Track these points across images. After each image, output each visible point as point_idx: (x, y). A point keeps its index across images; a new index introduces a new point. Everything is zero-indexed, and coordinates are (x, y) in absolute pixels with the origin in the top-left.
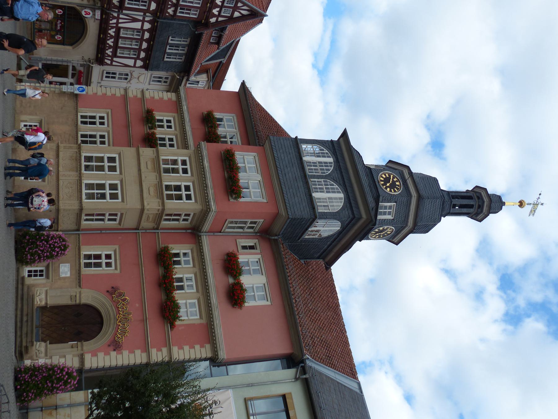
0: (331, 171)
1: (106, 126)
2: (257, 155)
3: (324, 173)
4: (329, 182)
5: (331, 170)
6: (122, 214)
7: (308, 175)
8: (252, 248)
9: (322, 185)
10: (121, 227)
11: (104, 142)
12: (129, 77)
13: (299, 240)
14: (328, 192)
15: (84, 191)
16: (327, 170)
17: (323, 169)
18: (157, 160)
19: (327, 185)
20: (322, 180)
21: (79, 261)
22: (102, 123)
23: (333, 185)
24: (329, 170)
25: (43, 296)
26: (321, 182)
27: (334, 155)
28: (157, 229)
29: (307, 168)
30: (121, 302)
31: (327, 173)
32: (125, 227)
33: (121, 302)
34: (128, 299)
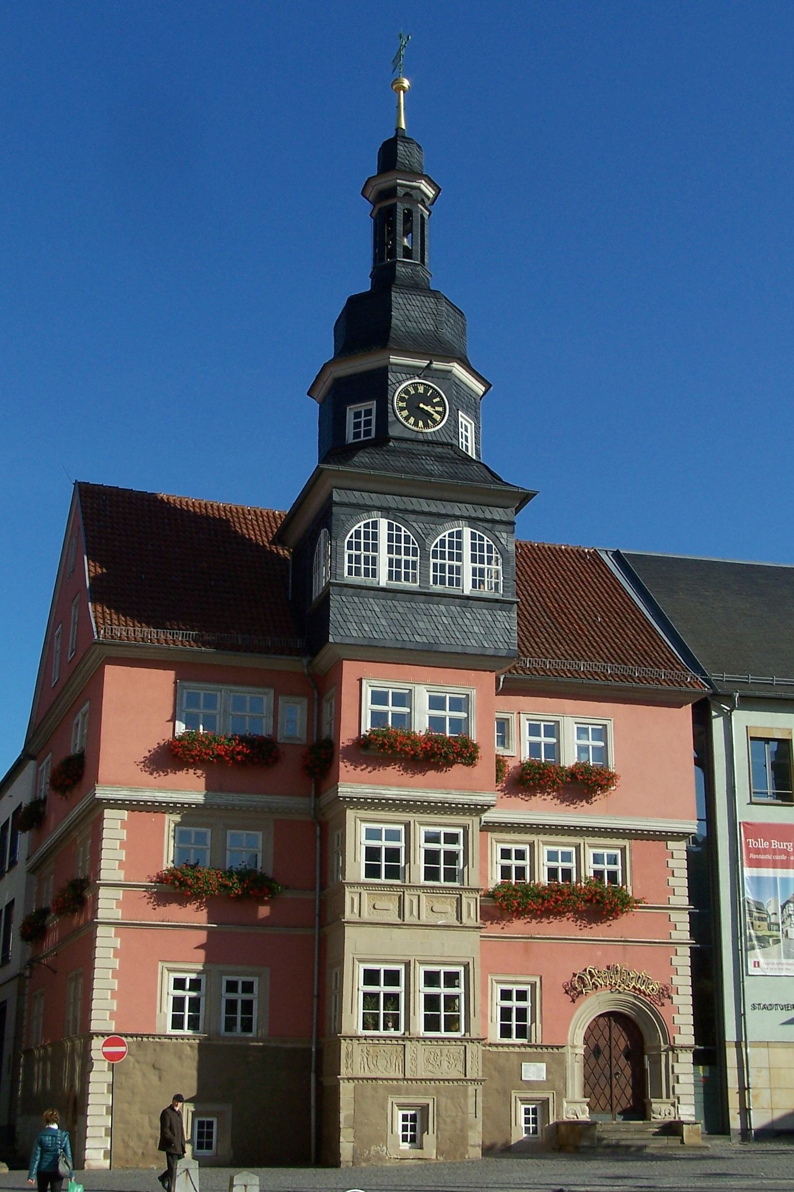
0: (409, 533)
2: (368, 681)
4: (436, 546)
5: (406, 530)
16: (407, 541)
20: (431, 559)
21: (513, 1045)
24: (407, 538)
25: (577, 1107)
27: (368, 511)
30: (595, 980)
31: (414, 543)
33: (595, 980)
34: (591, 968)
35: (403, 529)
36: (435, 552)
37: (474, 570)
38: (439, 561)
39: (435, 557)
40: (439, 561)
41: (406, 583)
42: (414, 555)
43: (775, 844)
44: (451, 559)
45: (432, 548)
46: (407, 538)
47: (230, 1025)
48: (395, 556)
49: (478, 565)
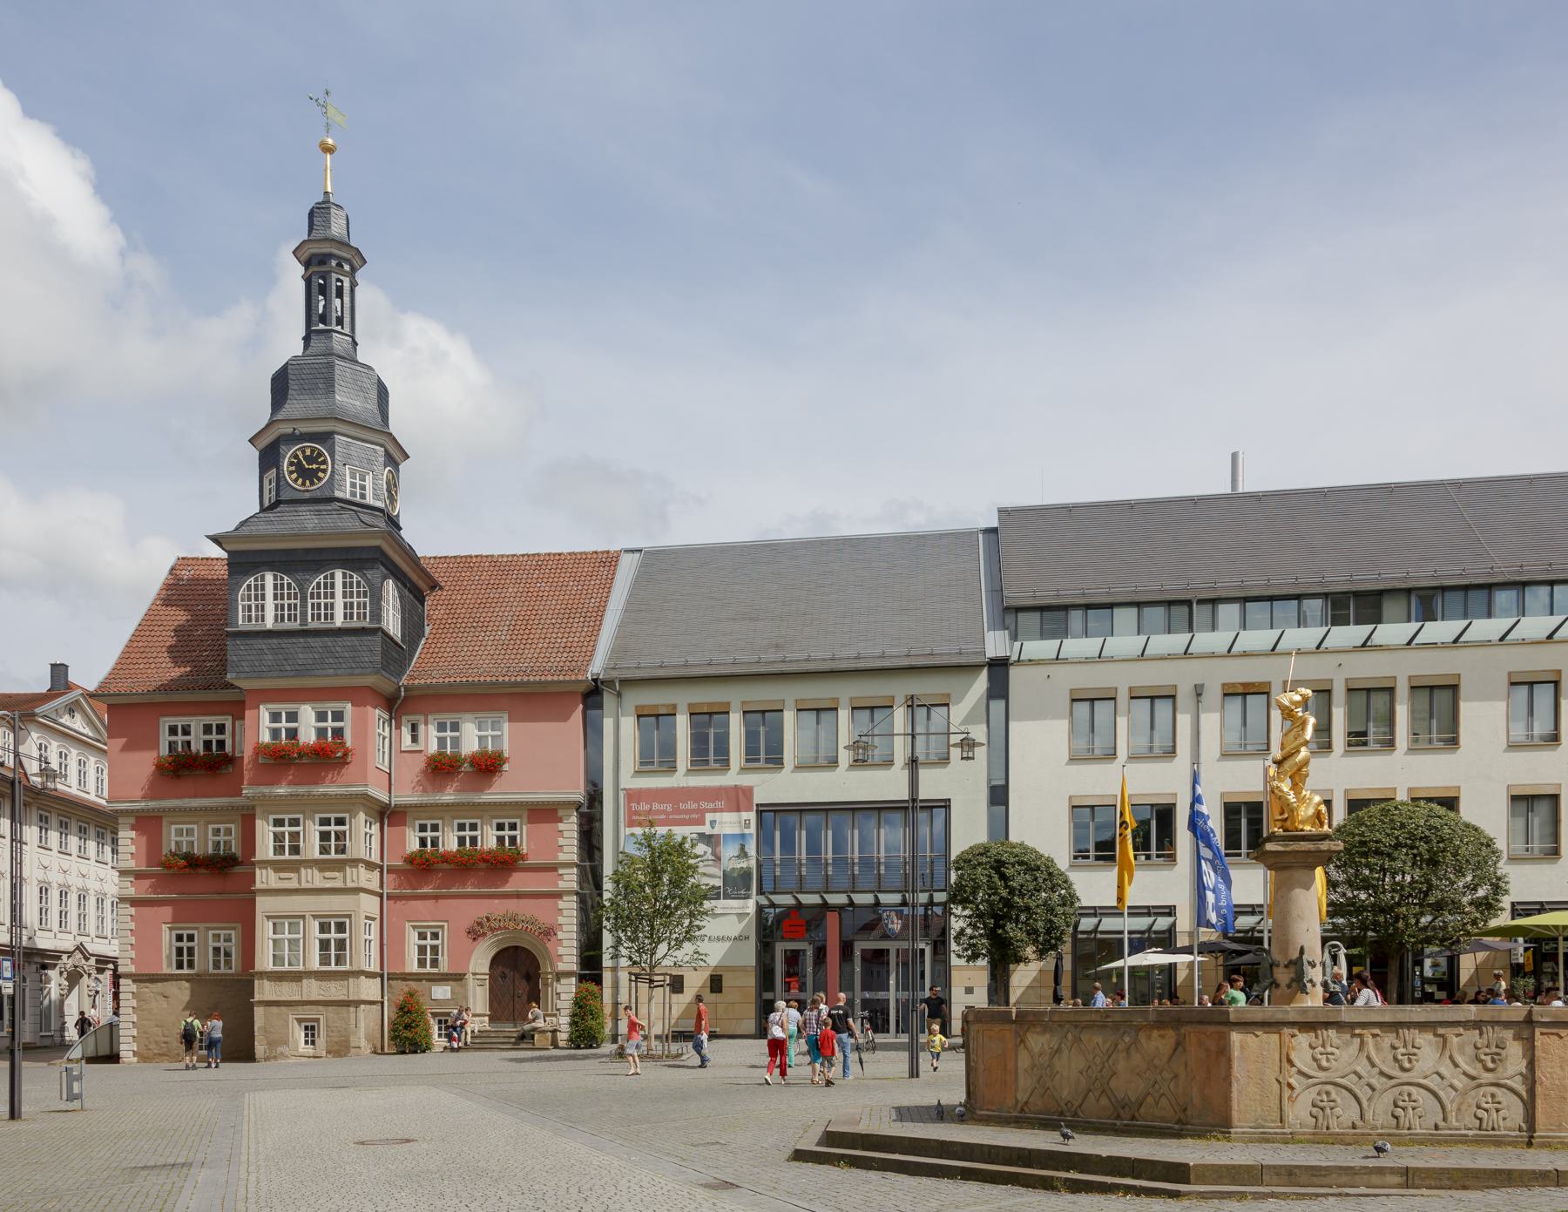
1: (195, 932)
3: (295, 594)
6: (367, 918)
7: (301, 625)
8: (414, 728)
9: (319, 604)
10: (378, 917)
11: (188, 935)
12: (44, 885)
13: (402, 648)
14: (333, 596)
15: (333, 967)
16: (289, 588)
17: (289, 594)
18: (278, 866)
19: (319, 594)
22: (191, 938)
23: (318, 584)
24: (289, 585)
26: (313, 604)
28: (381, 867)
29: (288, 625)
32: (379, 913)
35: (286, 578)
36: (312, 594)
37: (345, 604)
38: (315, 601)
39: (312, 598)
40: (315, 601)
41: (289, 624)
42: (296, 598)
43: (656, 806)
44: (326, 598)
45: (310, 590)
46: (289, 585)
47: (217, 965)
48: (279, 602)
49: (348, 600)
